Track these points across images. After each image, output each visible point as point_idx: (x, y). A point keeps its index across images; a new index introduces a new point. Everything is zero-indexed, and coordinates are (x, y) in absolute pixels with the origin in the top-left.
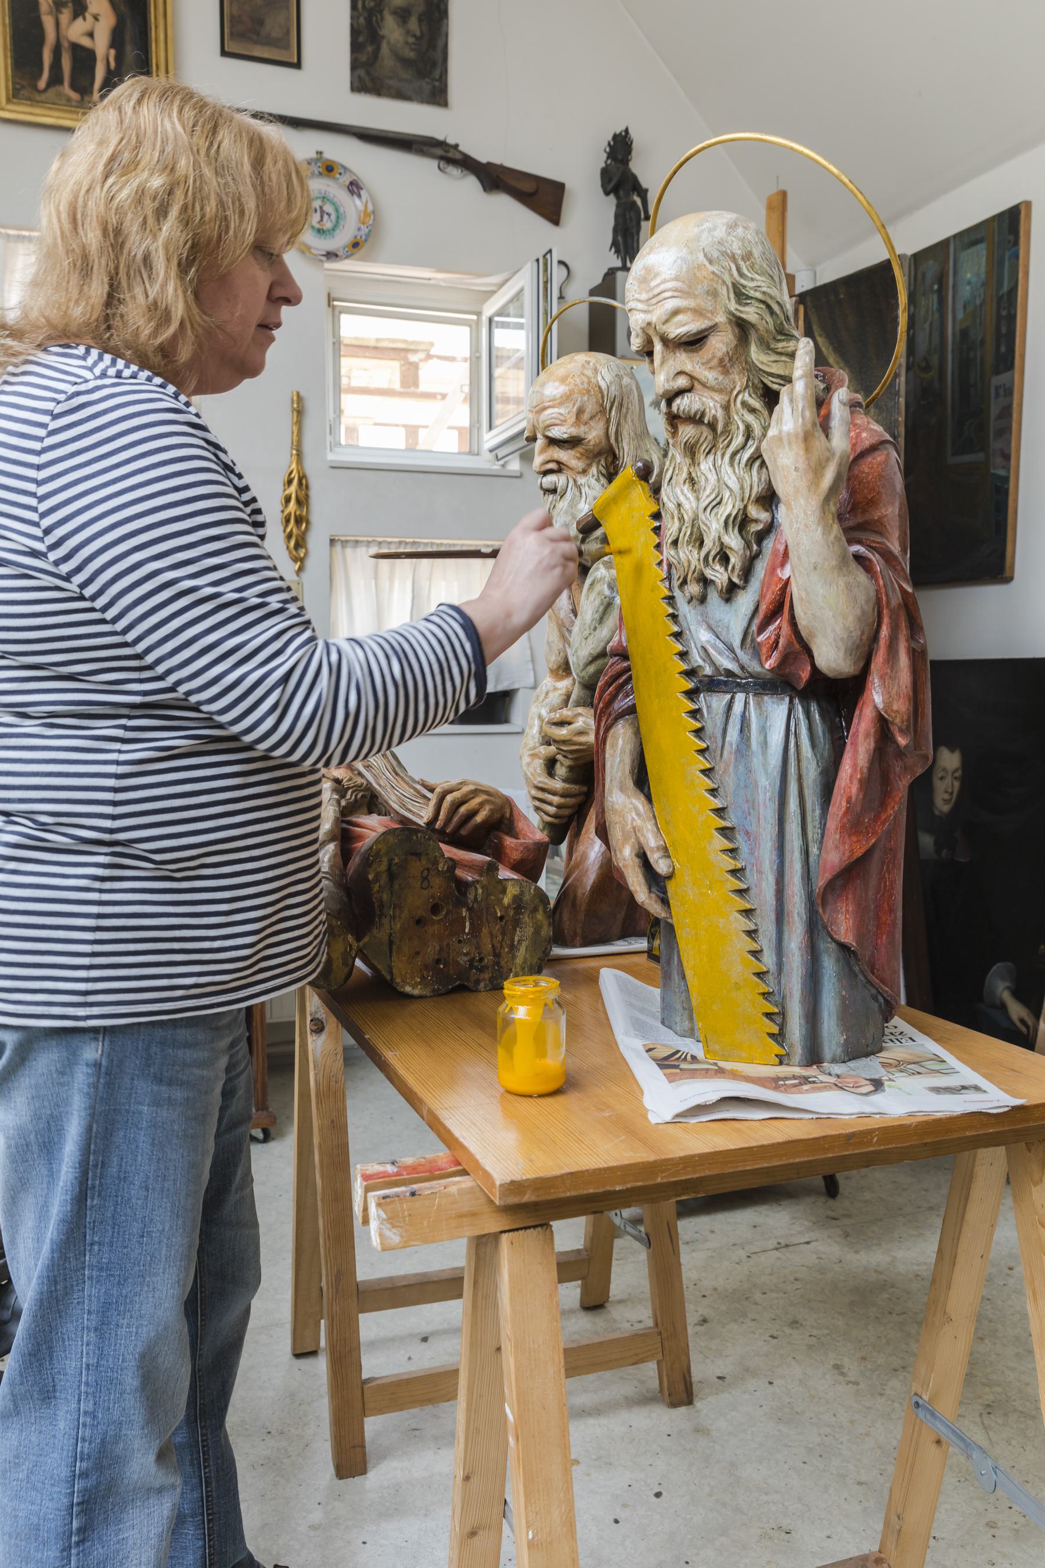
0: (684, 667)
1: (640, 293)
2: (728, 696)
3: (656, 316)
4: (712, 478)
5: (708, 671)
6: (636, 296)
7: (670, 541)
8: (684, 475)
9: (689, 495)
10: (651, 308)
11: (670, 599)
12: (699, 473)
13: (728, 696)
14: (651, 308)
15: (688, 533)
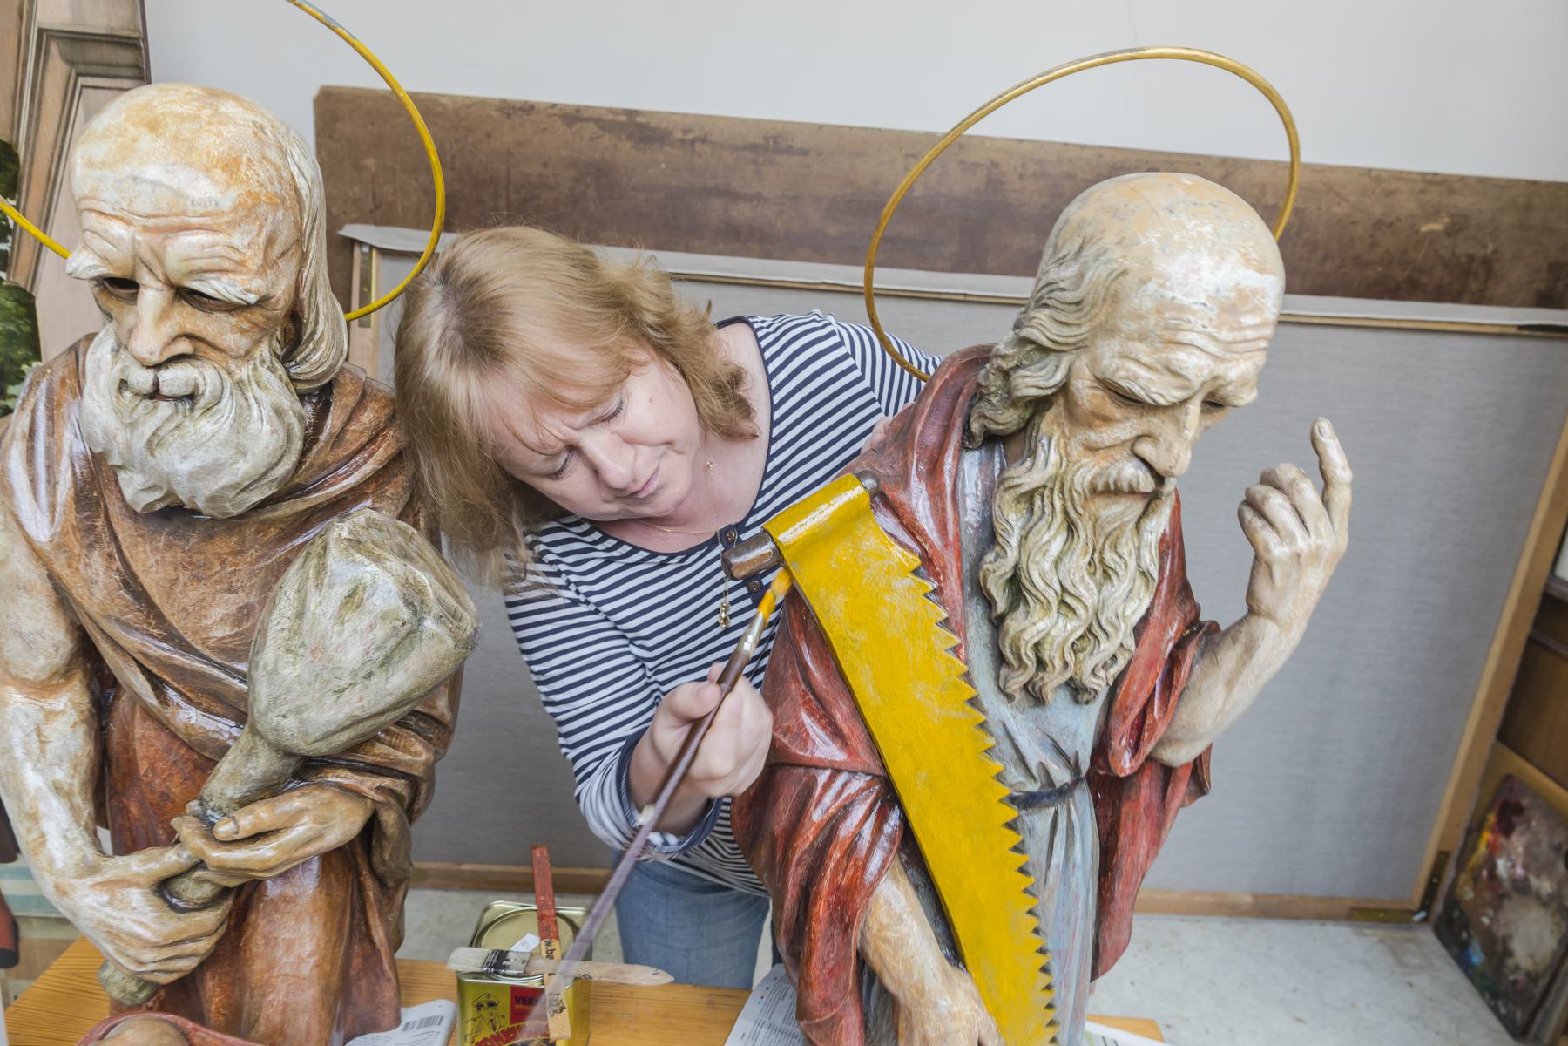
0: (1006, 791)
1: (1219, 327)
2: (1052, 810)
3: (1239, 370)
4: (1132, 564)
5: (1033, 787)
6: (1210, 330)
7: (1036, 639)
8: (1088, 559)
9: (1092, 585)
10: (1228, 356)
11: (974, 702)
12: (1109, 556)
13: (1052, 810)
14: (1228, 356)
15: (1079, 633)
